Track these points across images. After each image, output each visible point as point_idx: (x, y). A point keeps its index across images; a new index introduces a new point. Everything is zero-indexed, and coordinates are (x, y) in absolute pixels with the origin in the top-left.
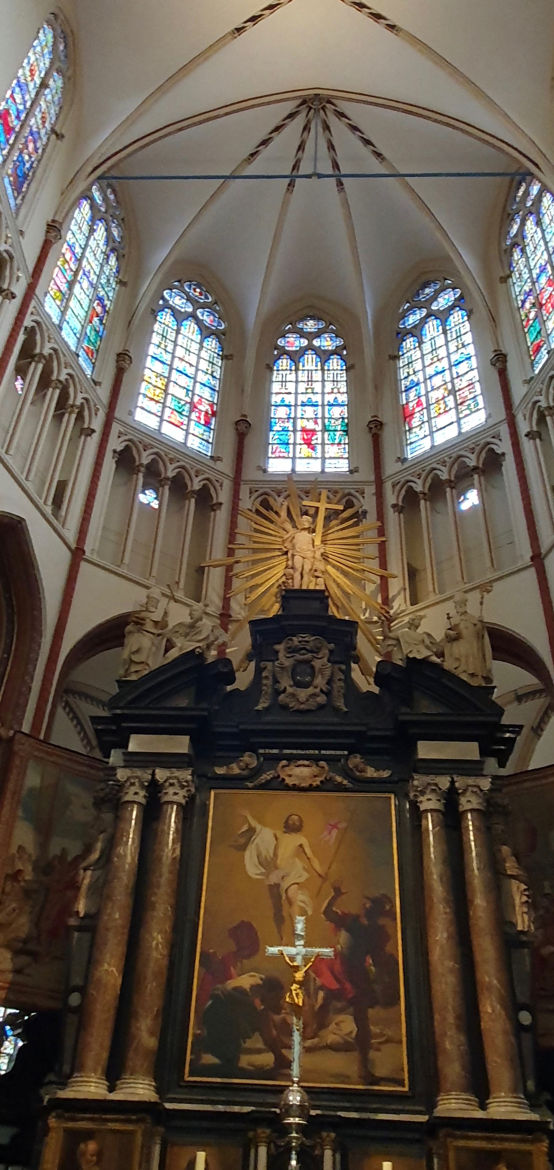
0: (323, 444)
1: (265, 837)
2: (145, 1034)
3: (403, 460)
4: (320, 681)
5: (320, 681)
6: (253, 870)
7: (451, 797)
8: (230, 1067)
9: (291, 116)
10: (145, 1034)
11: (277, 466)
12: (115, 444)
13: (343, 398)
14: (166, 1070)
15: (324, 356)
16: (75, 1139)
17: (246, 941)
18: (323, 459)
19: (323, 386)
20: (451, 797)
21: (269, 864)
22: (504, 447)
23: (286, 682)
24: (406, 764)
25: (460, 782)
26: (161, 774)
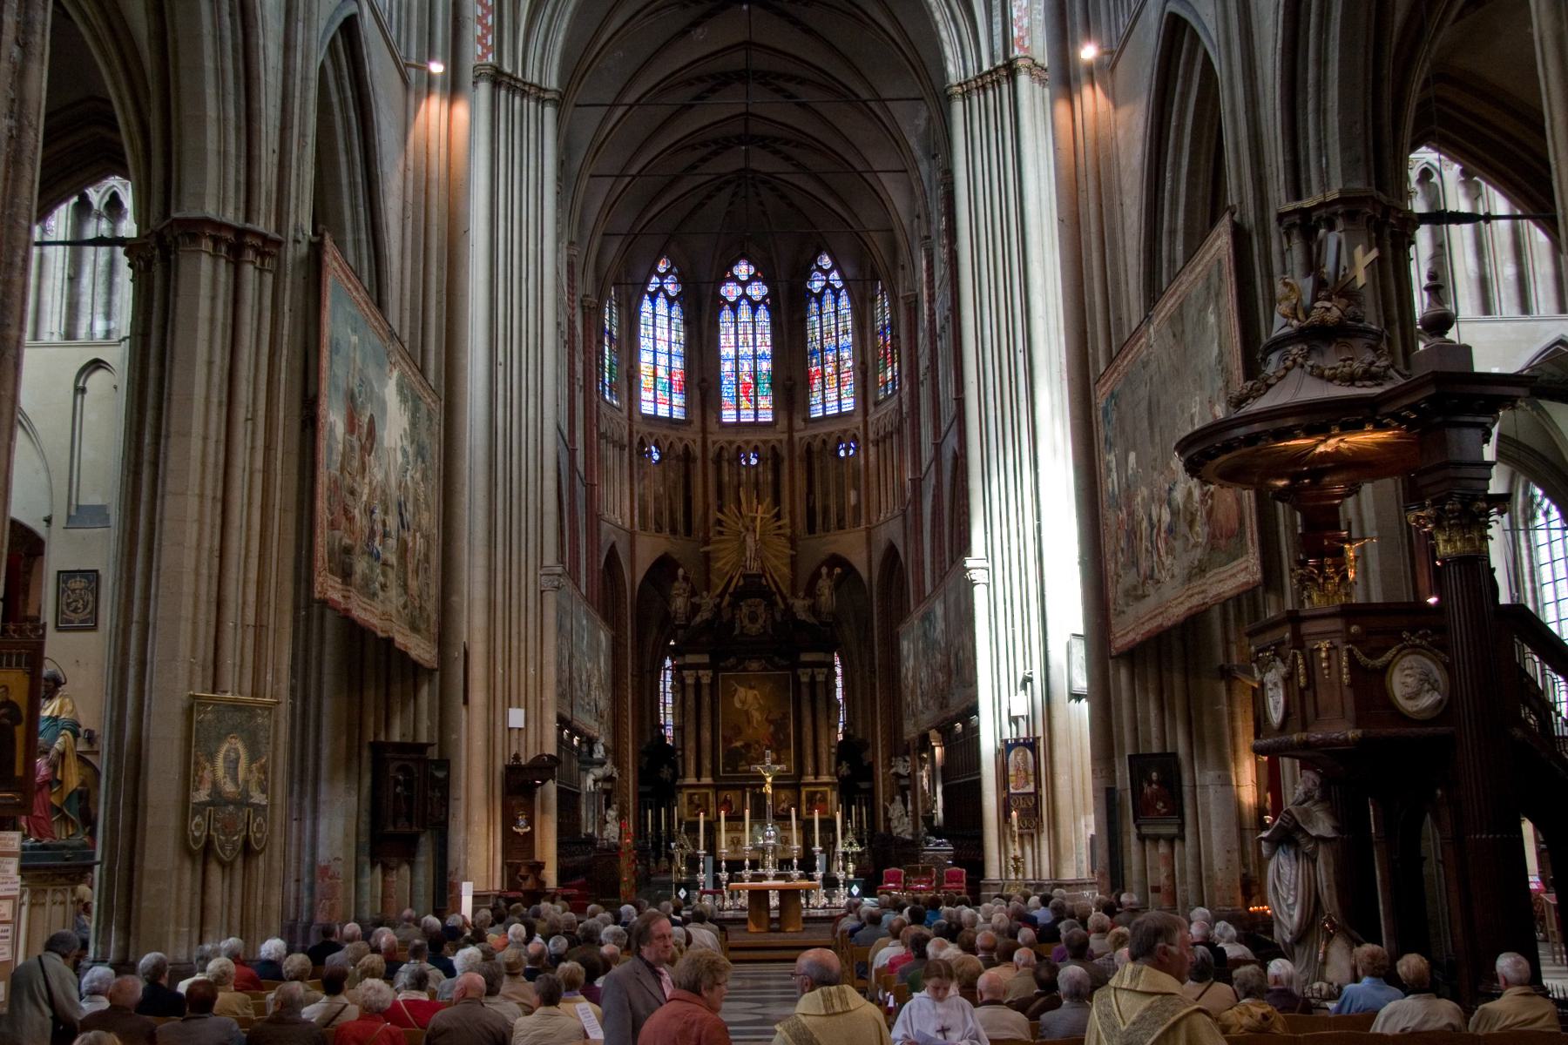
0: (756, 396)
1: (741, 691)
2: (707, 764)
3: (808, 420)
4: (761, 621)
5: (761, 621)
6: (738, 705)
7: (813, 677)
8: (735, 770)
9: (728, 182)
10: (707, 764)
11: (729, 416)
12: (636, 441)
13: (768, 351)
14: (714, 772)
15: (754, 306)
16: (691, 796)
17: (738, 731)
18: (756, 410)
19: (754, 340)
20: (813, 677)
21: (743, 702)
22: (860, 436)
23: (746, 622)
24: (796, 665)
25: (817, 670)
26: (701, 672)
